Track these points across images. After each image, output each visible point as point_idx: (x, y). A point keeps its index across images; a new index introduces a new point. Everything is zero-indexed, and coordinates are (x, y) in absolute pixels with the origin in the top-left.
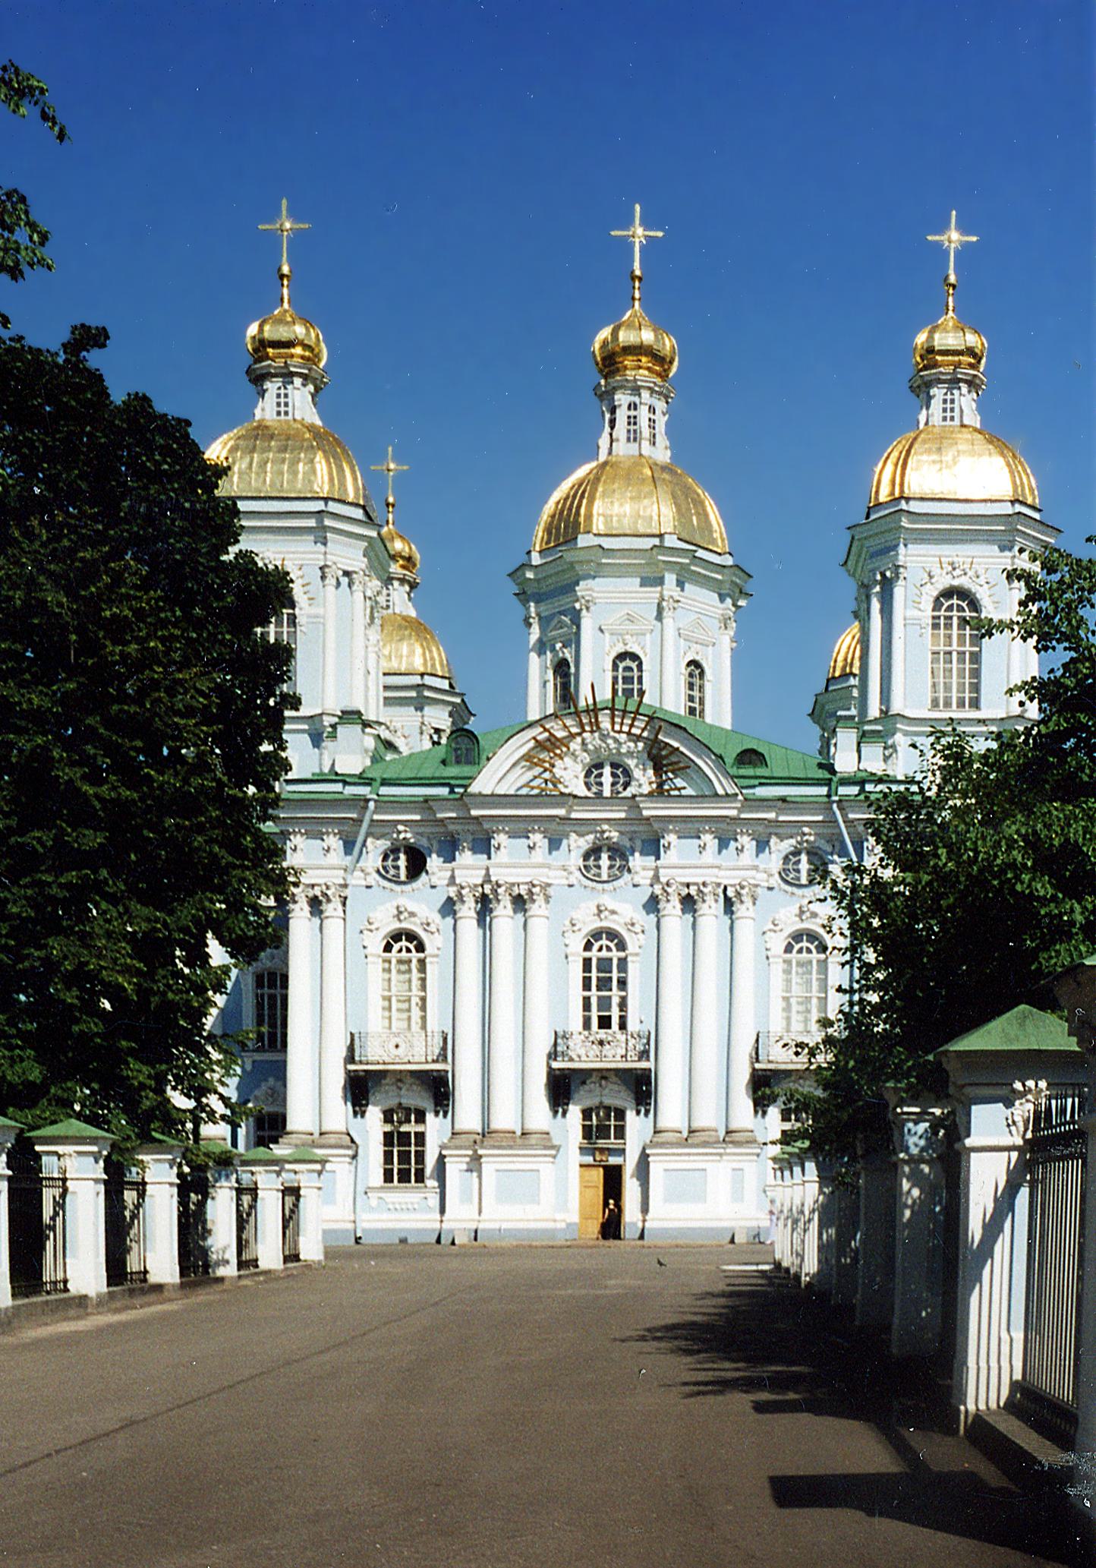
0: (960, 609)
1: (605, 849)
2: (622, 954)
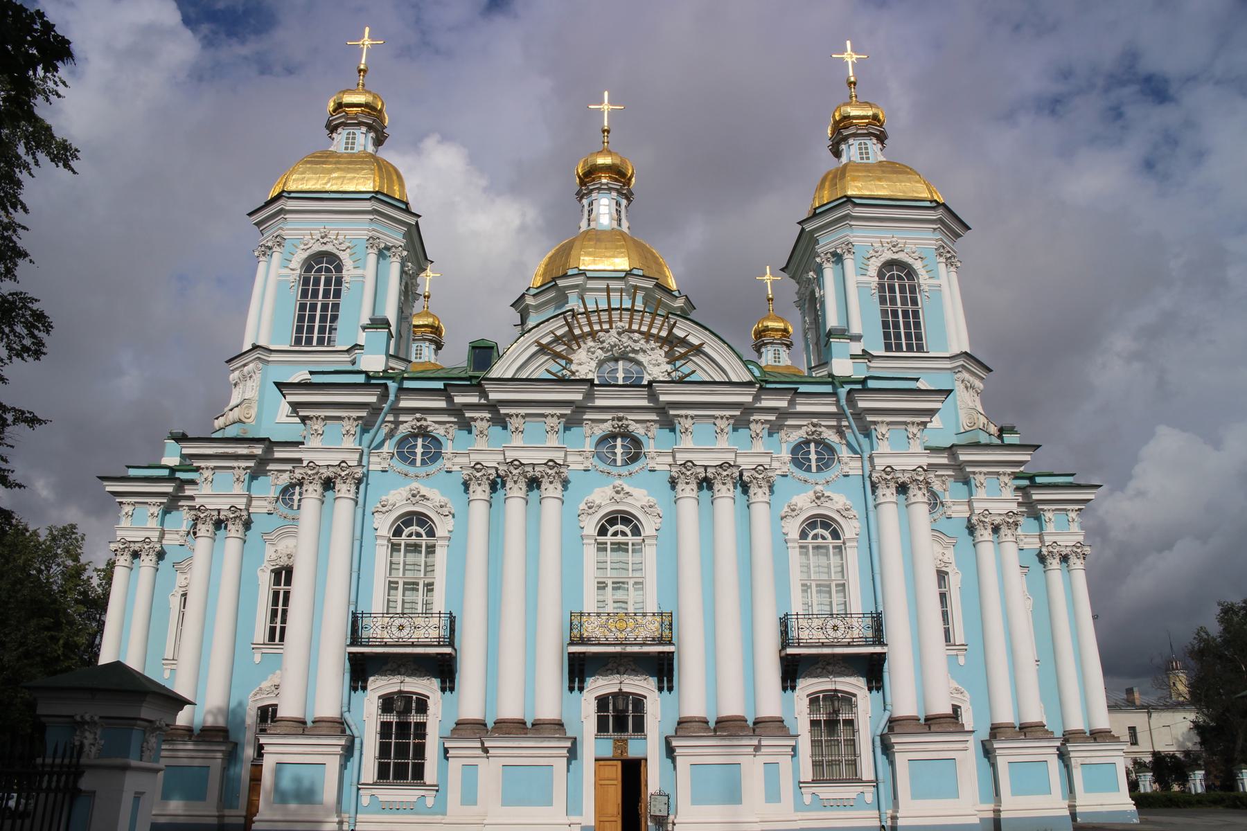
0: (900, 278)
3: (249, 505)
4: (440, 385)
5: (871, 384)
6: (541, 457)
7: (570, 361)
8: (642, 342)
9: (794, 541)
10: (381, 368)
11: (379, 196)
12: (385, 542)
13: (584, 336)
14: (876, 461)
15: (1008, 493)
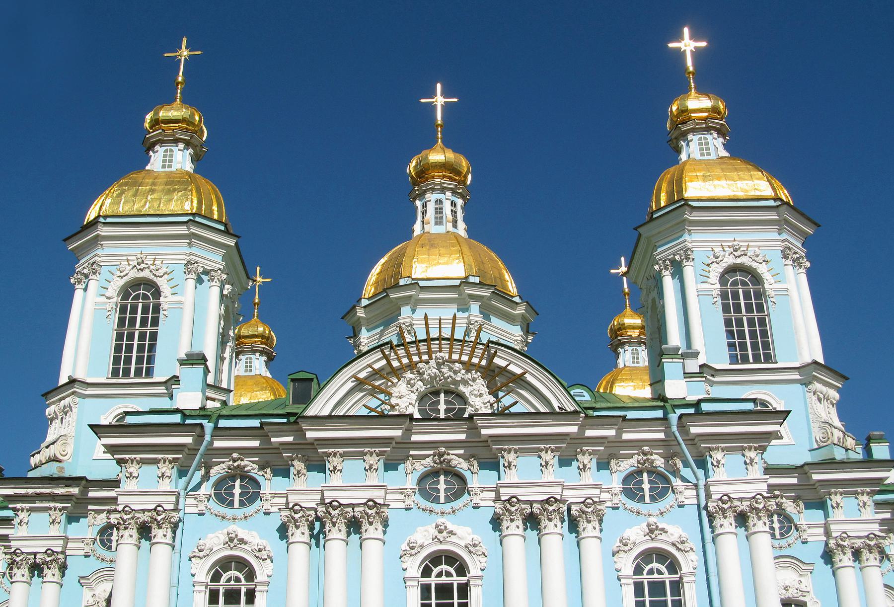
0: (744, 283)
1: (442, 472)
3: (65, 547)
4: (256, 423)
5: (705, 407)
6: (360, 497)
7: (390, 395)
8: (463, 372)
9: (628, 577)
10: (197, 406)
11: (198, 219)
12: (203, 588)
13: (402, 369)
14: (713, 489)
15: (869, 513)
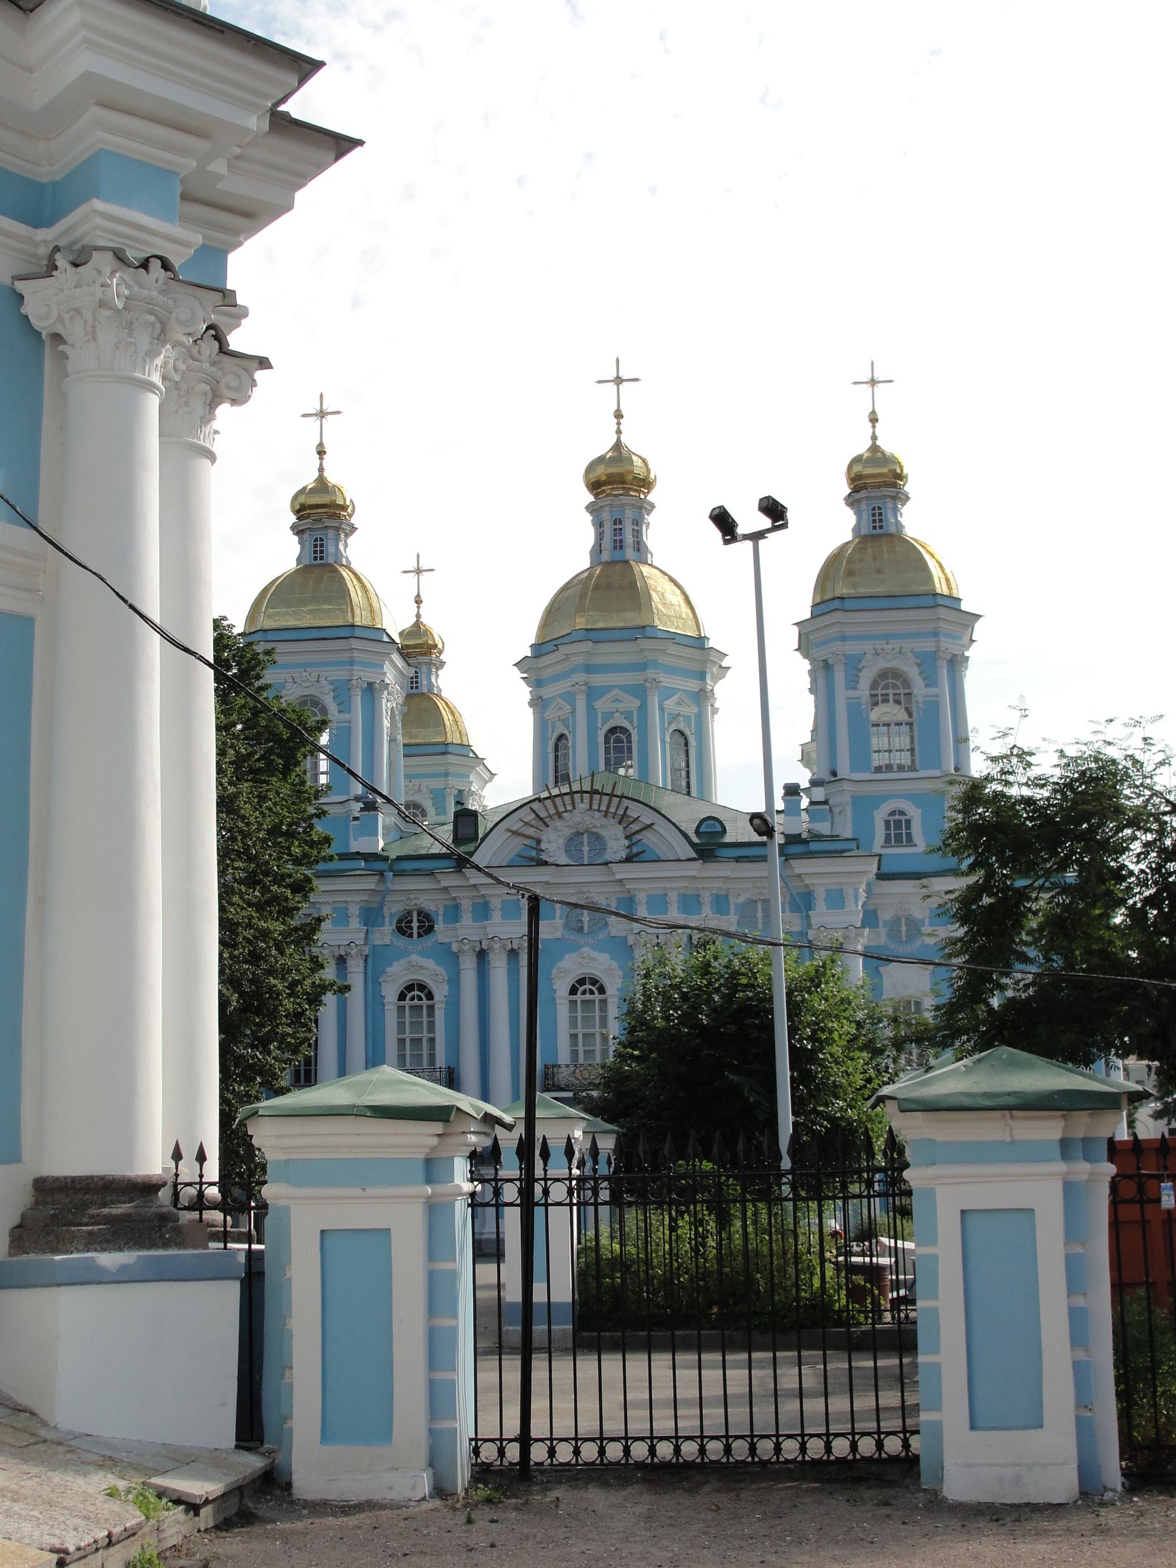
0: (895, 687)
2: (602, 997)
7: (539, 842)
